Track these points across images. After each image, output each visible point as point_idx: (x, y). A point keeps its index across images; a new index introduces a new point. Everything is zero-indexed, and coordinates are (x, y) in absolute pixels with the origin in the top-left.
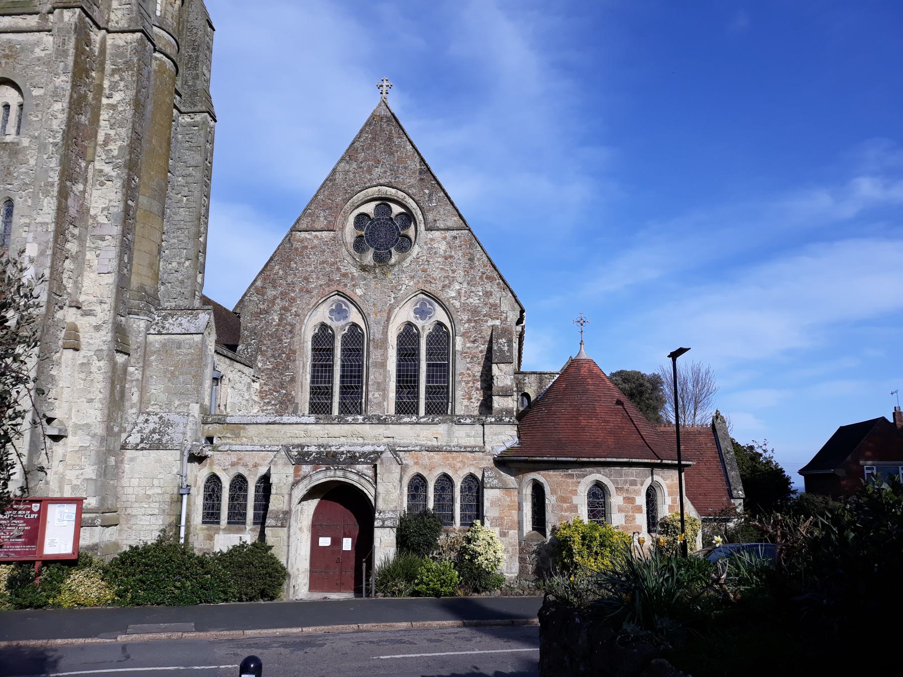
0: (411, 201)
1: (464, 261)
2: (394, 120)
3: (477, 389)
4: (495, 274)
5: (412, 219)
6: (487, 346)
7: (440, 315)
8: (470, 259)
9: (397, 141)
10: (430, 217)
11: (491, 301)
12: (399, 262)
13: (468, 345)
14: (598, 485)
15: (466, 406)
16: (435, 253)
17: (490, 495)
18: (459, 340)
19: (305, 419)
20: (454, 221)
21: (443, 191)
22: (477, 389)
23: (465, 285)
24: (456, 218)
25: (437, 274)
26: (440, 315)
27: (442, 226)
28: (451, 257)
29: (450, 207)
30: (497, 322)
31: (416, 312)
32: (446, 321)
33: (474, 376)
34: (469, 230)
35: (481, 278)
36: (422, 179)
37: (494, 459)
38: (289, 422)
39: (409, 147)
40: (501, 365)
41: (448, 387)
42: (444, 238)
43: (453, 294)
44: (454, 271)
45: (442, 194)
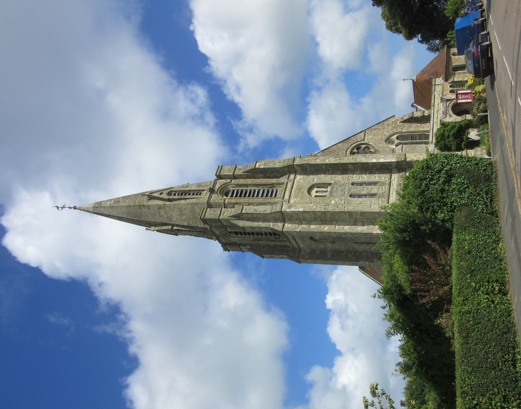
0: (353, 145)
1: (376, 131)
2: (324, 151)
3: (421, 125)
4: (382, 123)
5: (359, 146)
6: (406, 124)
7: (394, 137)
8: (376, 129)
9: (331, 150)
10: (359, 140)
11: (391, 123)
12: (373, 147)
13: (405, 128)
14: (452, 54)
15: (426, 128)
16: (372, 138)
17: (455, 80)
18: (404, 131)
19: (432, 112)
20: (362, 134)
21: (351, 137)
22: (421, 125)
23: (384, 130)
24: (361, 134)
25: (380, 137)
26: (394, 137)
27: (363, 137)
28: (374, 134)
29: (357, 135)
30: (398, 122)
31: (392, 144)
32: (396, 136)
33: (416, 126)
34: (366, 130)
35: (383, 126)
36: (346, 143)
37: (445, 82)
38: (432, 126)
39: (334, 147)
40: (414, 115)
41: (419, 135)
42: (367, 136)
43: (387, 133)
44: (379, 133)
45: (352, 138)
